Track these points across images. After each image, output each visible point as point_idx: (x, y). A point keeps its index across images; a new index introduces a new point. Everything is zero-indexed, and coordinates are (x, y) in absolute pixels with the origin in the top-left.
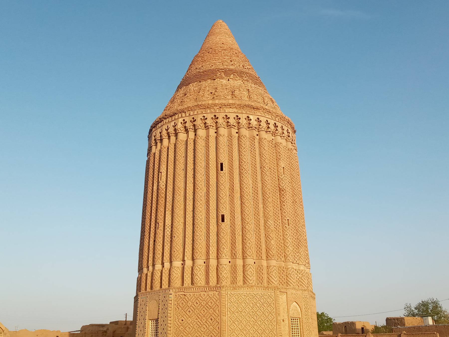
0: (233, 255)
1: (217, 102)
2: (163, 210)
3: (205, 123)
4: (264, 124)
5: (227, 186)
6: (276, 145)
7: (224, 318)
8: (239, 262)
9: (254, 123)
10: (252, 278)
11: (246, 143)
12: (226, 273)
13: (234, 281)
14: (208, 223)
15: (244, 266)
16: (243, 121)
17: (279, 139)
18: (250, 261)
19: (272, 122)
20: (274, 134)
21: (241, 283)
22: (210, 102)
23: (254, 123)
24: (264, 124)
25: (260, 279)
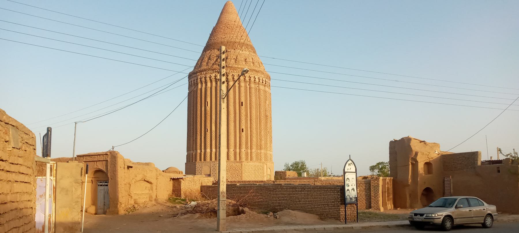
0: (247, 148)
1: (239, 66)
2: (209, 122)
3: (233, 78)
4: (261, 81)
5: (244, 113)
6: (265, 91)
7: (244, 175)
8: (249, 151)
9: (257, 80)
10: (254, 158)
11: (253, 91)
12: (243, 156)
13: (247, 159)
14: (235, 132)
15: (251, 153)
16: (252, 79)
17: (267, 89)
18: (253, 150)
19: (264, 79)
20: (265, 86)
21: (249, 160)
22: (236, 66)
23: (257, 80)
24: (261, 81)
25: (257, 159)
